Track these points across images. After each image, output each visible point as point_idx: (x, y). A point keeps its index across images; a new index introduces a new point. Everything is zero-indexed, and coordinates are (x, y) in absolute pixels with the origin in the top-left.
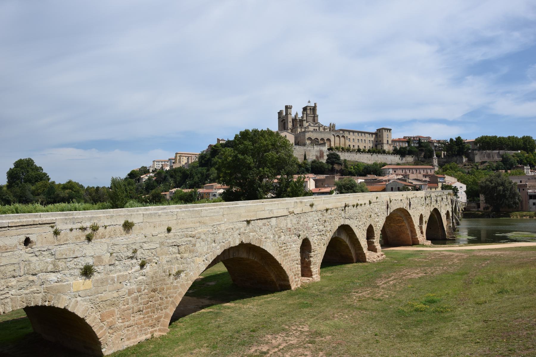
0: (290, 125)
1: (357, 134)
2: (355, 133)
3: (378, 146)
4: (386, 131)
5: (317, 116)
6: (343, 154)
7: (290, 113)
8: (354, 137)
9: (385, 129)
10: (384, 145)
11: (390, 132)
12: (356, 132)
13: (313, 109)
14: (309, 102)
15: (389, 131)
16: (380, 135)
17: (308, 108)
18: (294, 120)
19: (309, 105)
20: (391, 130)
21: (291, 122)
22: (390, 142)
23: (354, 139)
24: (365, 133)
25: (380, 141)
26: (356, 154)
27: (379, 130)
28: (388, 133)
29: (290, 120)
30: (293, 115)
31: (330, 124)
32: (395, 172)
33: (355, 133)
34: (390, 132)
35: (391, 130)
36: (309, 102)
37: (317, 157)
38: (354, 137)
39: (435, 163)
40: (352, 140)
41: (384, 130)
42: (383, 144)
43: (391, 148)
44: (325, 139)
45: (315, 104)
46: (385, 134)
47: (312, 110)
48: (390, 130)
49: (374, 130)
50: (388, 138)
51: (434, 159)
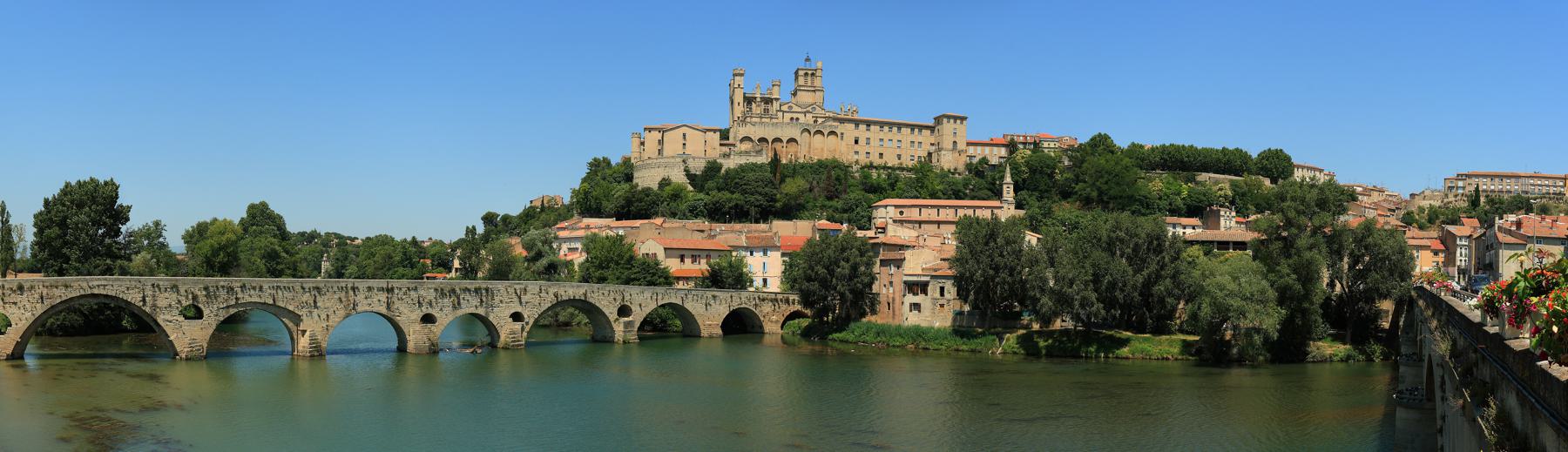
4: (952, 121)
8: (868, 134)
9: (949, 117)
11: (962, 123)
12: (875, 123)
13: (813, 74)
14: (808, 60)
15: (958, 121)
17: (801, 73)
21: (741, 104)
22: (961, 146)
23: (868, 139)
24: (900, 126)
32: (901, 213)
34: (962, 123)
39: (1008, 195)
40: (862, 141)
41: (945, 120)
44: (785, 140)
47: (809, 78)
48: (963, 119)
49: (931, 123)
51: (1005, 186)
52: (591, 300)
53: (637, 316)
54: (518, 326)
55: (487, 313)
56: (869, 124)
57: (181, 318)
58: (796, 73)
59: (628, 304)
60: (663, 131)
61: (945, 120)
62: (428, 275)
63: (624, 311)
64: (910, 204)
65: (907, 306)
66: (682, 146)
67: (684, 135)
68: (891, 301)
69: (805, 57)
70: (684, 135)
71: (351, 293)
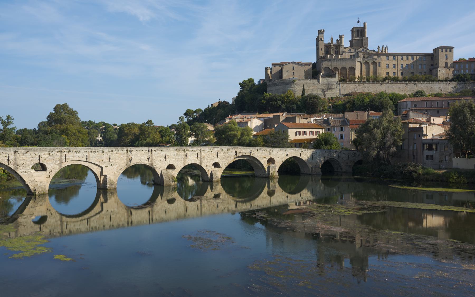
0: (322, 53)
1: (400, 57)
2: (396, 57)
3: (433, 71)
4: (444, 50)
5: (367, 39)
6: (361, 85)
7: (322, 39)
8: (395, 62)
9: (442, 48)
10: (439, 69)
14: (358, 22)
15: (448, 50)
16: (436, 57)
18: (328, 48)
19: (359, 25)
20: (453, 48)
21: (323, 50)
23: (394, 65)
25: (436, 64)
26: (382, 84)
27: (436, 50)
28: (448, 53)
29: (321, 46)
30: (326, 40)
31: (378, 47)
33: (396, 57)
34: (451, 51)
35: (453, 48)
36: (358, 22)
37: (323, 91)
38: (395, 62)
40: (391, 66)
42: (438, 67)
43: (450, 73)
45: (364, 24)
46: (442, 55)
48: (451, 48)
49: (431, 52)
50: (447, 59)
52: (254, 156)
53: (278, 164)
54: (217, 169)
55: (201, 163)
56: (394, 55)
57: (33, 171)
58: (352, 30)
59: (272, 157)
60: (282, 65)
61: (440, 50)
62: (160, 144)
63: (271, 161)
64: (449, 99)
65: (425, 157)
66: (292, 73)
67: (293, 69)
68: (415, 154)
69: (357, 21)
70: (293, 69)
71: (129, 153)
